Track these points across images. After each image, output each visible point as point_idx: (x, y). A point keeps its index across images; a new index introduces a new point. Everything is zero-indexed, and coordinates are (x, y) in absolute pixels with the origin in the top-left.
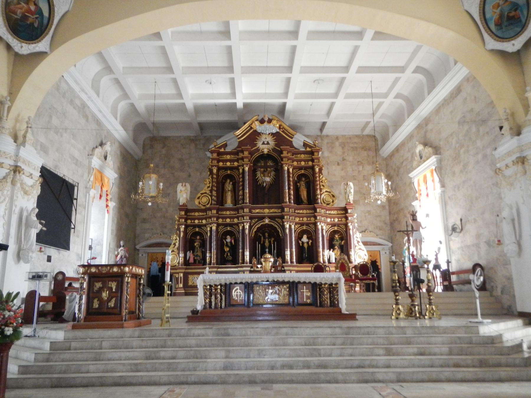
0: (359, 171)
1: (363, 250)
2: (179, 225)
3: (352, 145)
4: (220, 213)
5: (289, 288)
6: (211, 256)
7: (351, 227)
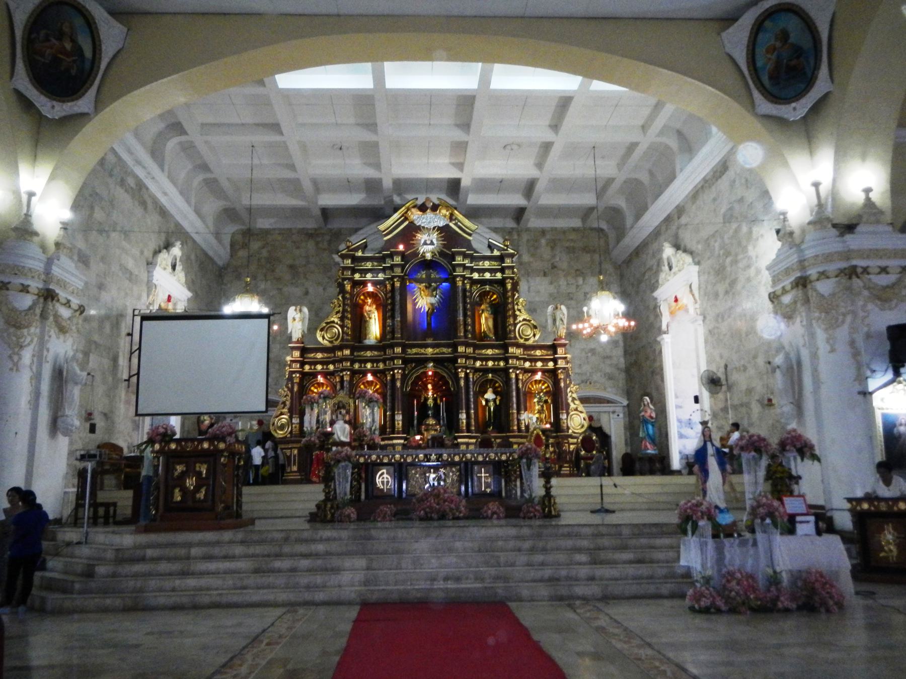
0: (578, 286)
1: (581, 412)
3: (567, 244)
4: (355, 354)
5: (460, 470)
7: (562, 376)
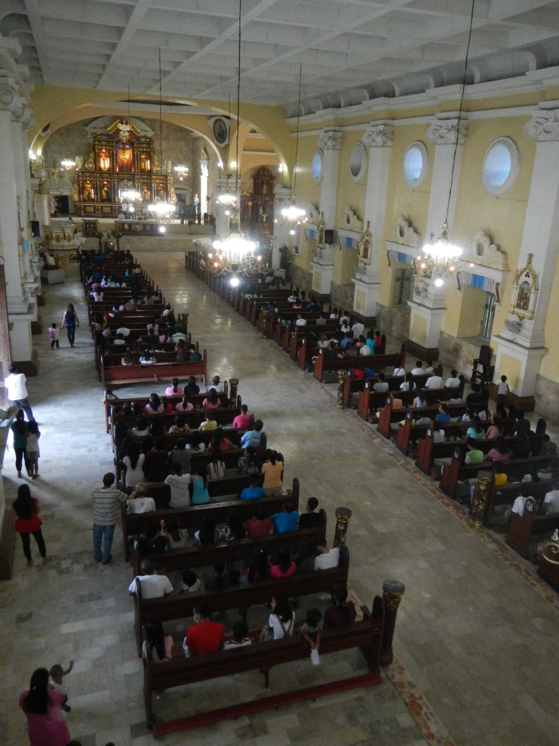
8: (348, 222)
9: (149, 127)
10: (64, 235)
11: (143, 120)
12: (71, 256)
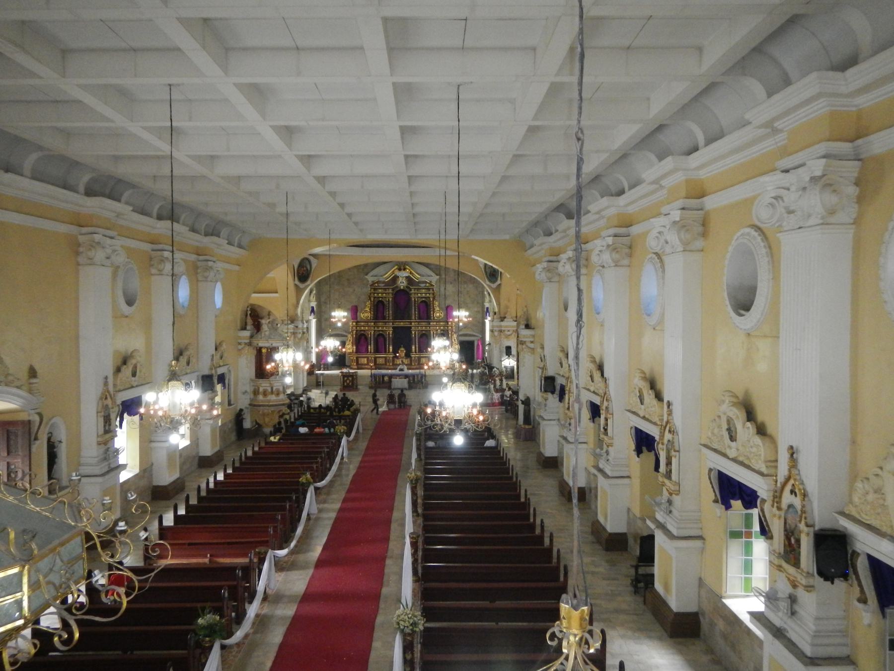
2: (352, 331)
6: (371, 348)
8: (561, 364)
9: (433, 272)
10: (272, 388)
11: (427, 265)
12: (279, 411)
